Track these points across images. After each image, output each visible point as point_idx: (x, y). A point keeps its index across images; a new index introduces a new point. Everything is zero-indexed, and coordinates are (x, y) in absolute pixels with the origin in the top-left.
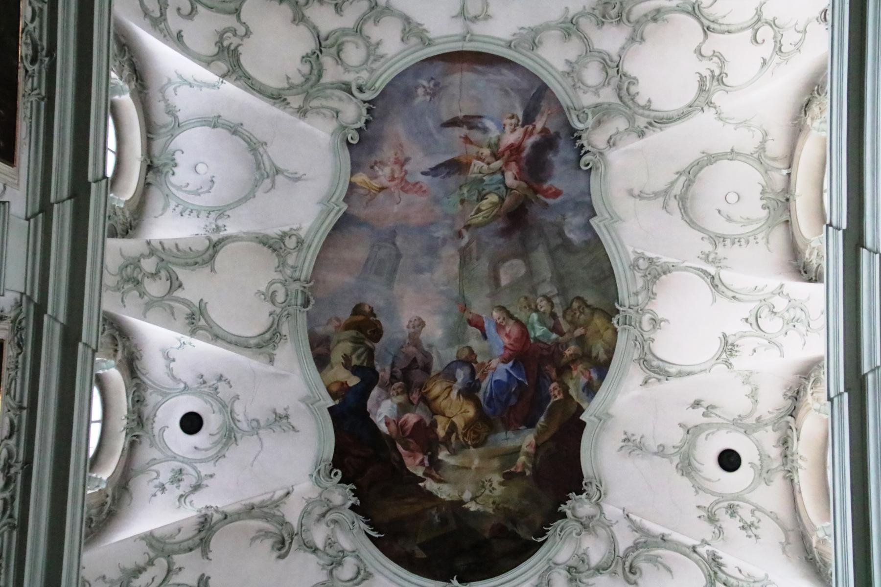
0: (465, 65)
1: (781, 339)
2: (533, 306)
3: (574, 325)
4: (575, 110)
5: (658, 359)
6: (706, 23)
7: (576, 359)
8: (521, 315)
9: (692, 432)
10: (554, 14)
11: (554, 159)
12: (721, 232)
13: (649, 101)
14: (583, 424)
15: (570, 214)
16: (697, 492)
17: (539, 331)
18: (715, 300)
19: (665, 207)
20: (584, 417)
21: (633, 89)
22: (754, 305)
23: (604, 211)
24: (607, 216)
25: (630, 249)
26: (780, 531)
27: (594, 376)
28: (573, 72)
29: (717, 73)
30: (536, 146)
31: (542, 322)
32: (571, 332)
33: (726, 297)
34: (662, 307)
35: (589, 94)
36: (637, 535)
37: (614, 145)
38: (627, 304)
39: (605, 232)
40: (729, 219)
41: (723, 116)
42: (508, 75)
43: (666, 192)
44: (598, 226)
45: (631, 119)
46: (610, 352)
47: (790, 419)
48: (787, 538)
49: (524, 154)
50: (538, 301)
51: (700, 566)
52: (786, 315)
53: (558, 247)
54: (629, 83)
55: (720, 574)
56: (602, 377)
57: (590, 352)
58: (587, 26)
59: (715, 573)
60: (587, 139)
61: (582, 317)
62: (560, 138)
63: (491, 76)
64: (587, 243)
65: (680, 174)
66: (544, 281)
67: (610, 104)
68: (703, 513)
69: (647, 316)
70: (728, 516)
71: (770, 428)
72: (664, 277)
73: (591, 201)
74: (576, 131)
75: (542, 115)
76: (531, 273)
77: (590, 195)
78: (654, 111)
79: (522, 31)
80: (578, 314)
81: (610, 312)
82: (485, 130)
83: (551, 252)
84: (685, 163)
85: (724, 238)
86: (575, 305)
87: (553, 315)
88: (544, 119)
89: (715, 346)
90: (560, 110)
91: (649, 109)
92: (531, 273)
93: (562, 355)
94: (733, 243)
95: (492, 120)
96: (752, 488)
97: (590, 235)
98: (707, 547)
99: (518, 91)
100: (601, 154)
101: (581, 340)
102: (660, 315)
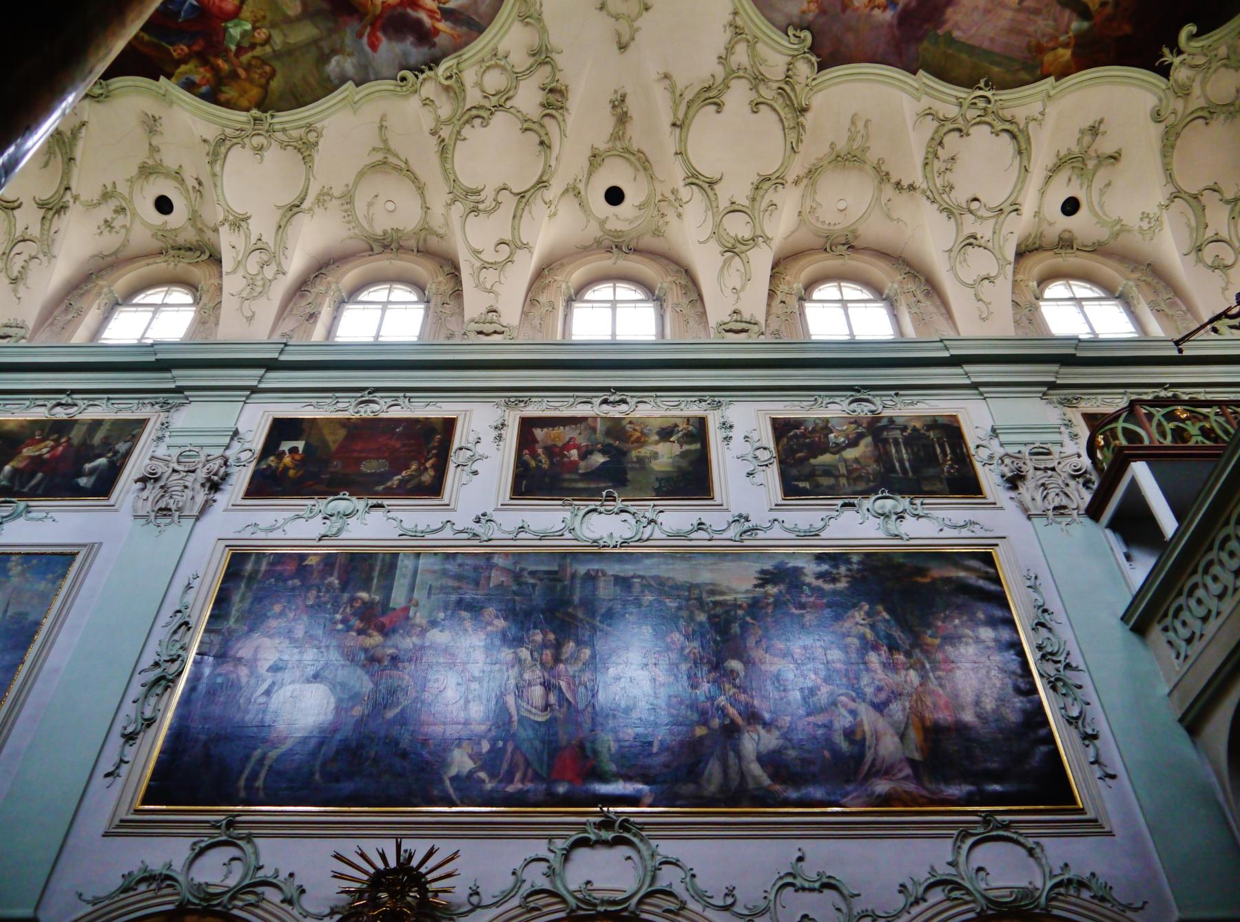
1: (241, 272)
2: (258, 25)
3: (248, 68)
4: (458, 64)
5: (227, 153)
6: (528, 195)
7: (215, 70)
8: (246, 12)
9: (178, 176)
11: (408, 42)
12: (356, 200)
13: (465, 139)
14: (157, 79)
15: (355, 62)
16: (128, 180)
17: (235, 31)
18: (279, 207)
20: (162, 78)
21: (477, 122)
22: (272, 245)
23: (361, 95)
24: (357, 98)
25: (325, 123)
26: (113, 250)
27: (204, 89)
28: (496, 60)
29: (481, 206)
30: (419, 22)
31: (244, 34)
32: (241, 65)
33: (281, 219)
34: (273, 154)
35: (475, 77)
36: (69, 134)
37: (425, 105)
38: (273, 121)
39: (341, 97)
40: (370, 205)
43: (389, 150)
44: (345, 90)
45: (448, 122)
46: (228, 105)
47: (208, 254)
48: (107, 256)
49: (409, 11)
50: (264, 30)
51: (55, 193)
52: (259, 278)
53: (320, 49)
54: (483, 118)
55: (51, 213)
56: (203, 97)
57: (226, 85)
58: (543, 74)
59: (51, 209)
60: (429, 78)
61: (257, 76)
62: (430, 48)
64: (328, 79)
65: (406, 163)
66: (285, 36)
67: (464, 99)
68: (109, 189)
69: (265, 142)
70: (113, 208)
71: (198, 238)
72: (301, 157)
73: (370, 81)
74: (437, 64)
75: (452, 28)
76: (289, 21)
77: (377, 80)
78: (455, 144)
79: (538, 4)
80: (259, 71)
81: (263, 105)
83: (315, 42)
85: (350, 201)
86: (268, 69)
87: (253, 46)
88: (448, 30)
89: (240, 209)
91: (457, 139)
92: (289, 21)
93: (217, 56)
94: (346, 211)
96: (146, 225)
97: (336, 82)
98: (71, 201)
100: (416, 92)
101: (234, 75)
102: (268, 154)
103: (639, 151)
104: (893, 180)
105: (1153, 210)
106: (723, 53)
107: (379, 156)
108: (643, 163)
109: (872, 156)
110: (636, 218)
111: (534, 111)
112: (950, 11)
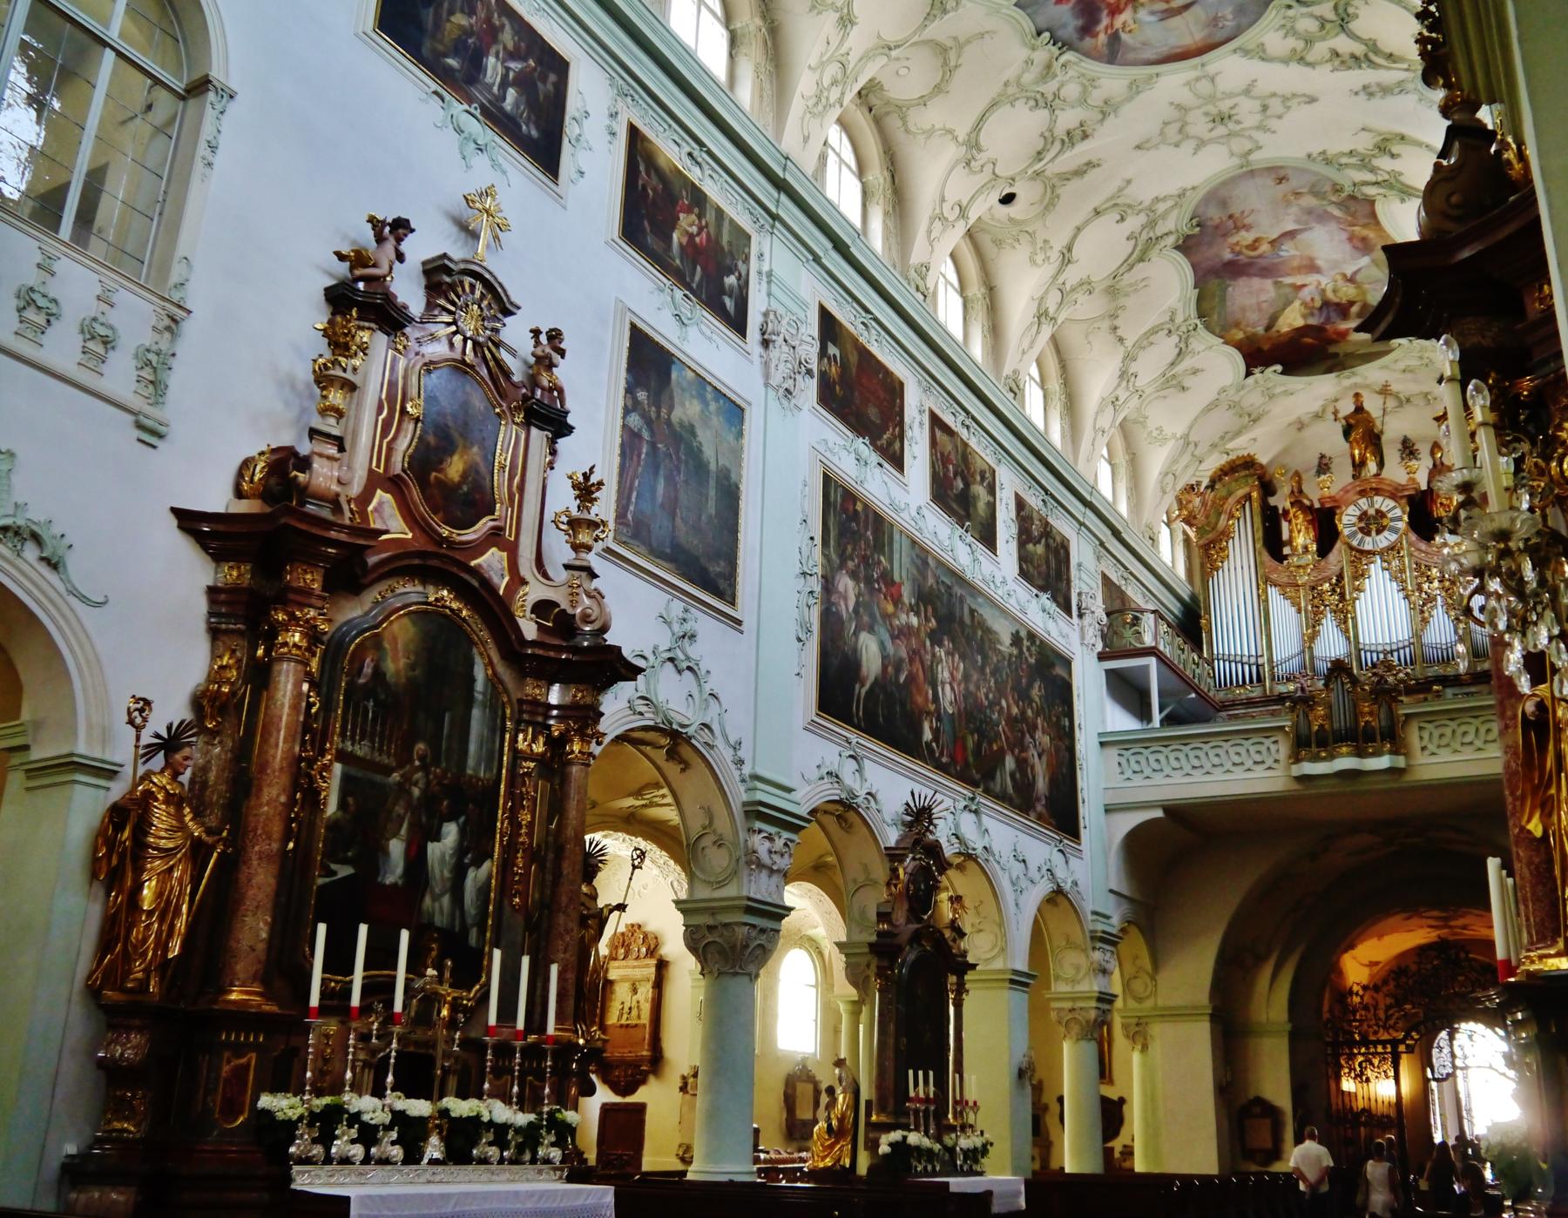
0: (1194, 47)
10: (1126, 109)
13: (1013, 106)
18: (879, 36)
19: (955, 39)
23: (1009, 12)
24: (1004, 11)
30: (1097, 21)
41: (950, 136)
42: (1149, 54)
49: (1105, 12)
63: (1165, 49)
82: (1152, 13)
84: (959, 75)
90: (1087, 54)
95: (1150, 23)
99: (1134, 49)
100: (1034, 49)
103: (1058, 196)
104: (1117, 323)
105: (1168, 431)
106: (1162, 196)
107: (949, 43)
108: (1050, 202)
109: (1122, 301)
110: (999, 221)
111: (1060, 131)
112: (1244, 278)
